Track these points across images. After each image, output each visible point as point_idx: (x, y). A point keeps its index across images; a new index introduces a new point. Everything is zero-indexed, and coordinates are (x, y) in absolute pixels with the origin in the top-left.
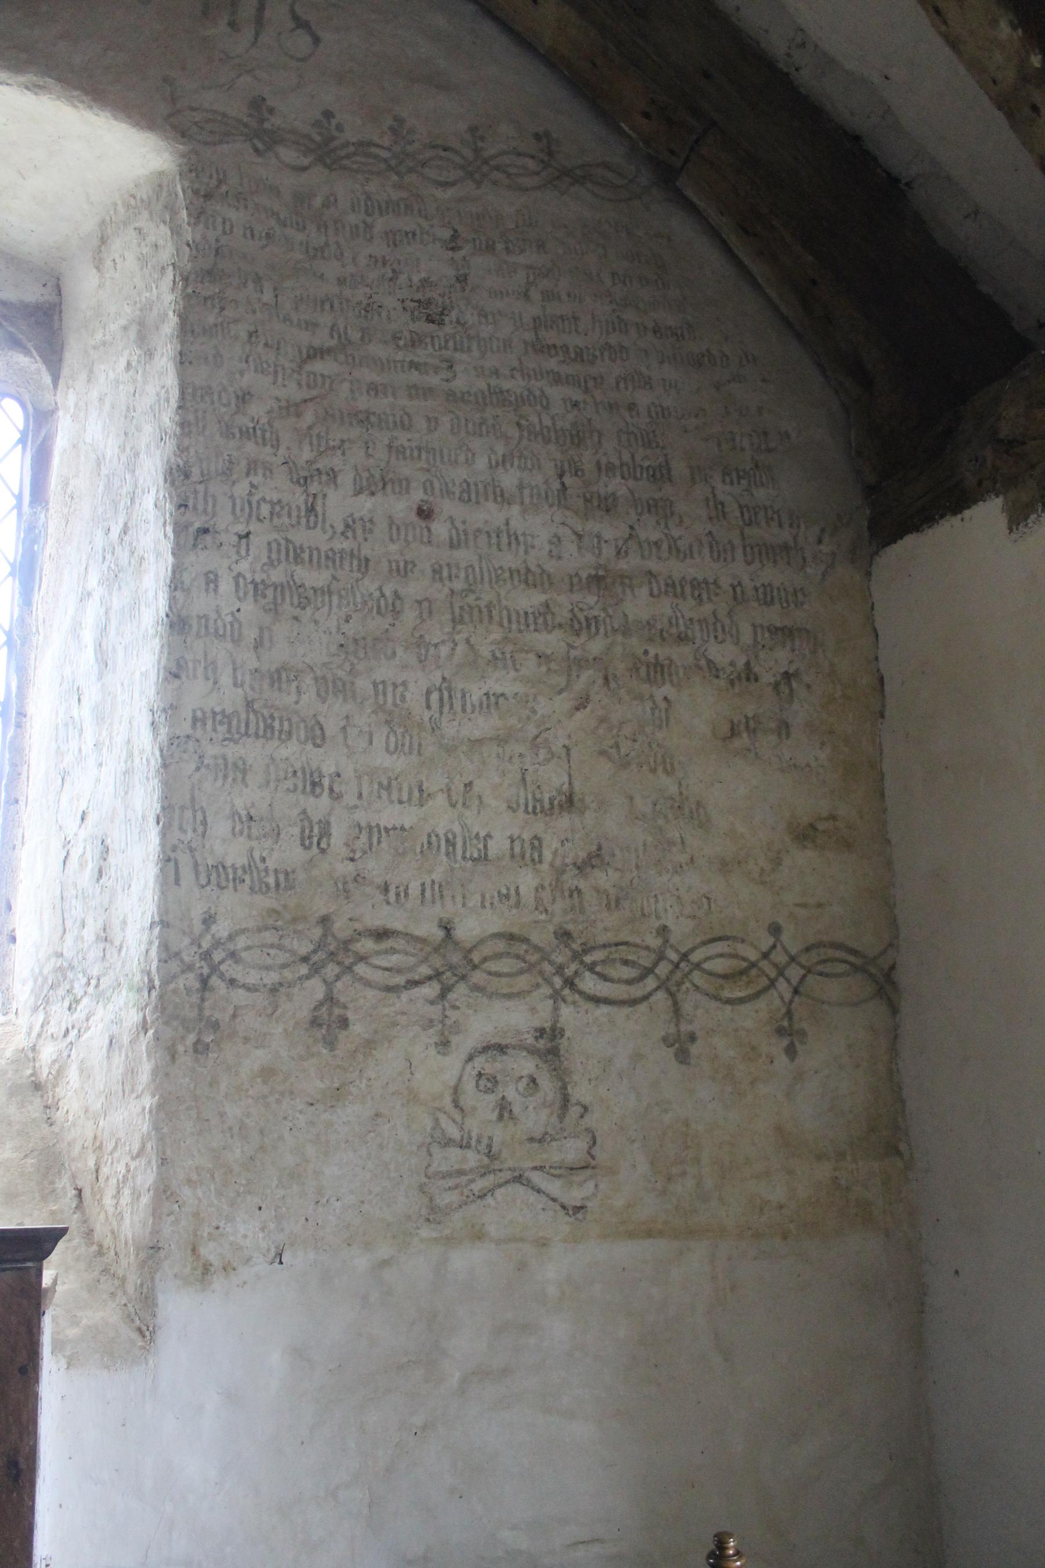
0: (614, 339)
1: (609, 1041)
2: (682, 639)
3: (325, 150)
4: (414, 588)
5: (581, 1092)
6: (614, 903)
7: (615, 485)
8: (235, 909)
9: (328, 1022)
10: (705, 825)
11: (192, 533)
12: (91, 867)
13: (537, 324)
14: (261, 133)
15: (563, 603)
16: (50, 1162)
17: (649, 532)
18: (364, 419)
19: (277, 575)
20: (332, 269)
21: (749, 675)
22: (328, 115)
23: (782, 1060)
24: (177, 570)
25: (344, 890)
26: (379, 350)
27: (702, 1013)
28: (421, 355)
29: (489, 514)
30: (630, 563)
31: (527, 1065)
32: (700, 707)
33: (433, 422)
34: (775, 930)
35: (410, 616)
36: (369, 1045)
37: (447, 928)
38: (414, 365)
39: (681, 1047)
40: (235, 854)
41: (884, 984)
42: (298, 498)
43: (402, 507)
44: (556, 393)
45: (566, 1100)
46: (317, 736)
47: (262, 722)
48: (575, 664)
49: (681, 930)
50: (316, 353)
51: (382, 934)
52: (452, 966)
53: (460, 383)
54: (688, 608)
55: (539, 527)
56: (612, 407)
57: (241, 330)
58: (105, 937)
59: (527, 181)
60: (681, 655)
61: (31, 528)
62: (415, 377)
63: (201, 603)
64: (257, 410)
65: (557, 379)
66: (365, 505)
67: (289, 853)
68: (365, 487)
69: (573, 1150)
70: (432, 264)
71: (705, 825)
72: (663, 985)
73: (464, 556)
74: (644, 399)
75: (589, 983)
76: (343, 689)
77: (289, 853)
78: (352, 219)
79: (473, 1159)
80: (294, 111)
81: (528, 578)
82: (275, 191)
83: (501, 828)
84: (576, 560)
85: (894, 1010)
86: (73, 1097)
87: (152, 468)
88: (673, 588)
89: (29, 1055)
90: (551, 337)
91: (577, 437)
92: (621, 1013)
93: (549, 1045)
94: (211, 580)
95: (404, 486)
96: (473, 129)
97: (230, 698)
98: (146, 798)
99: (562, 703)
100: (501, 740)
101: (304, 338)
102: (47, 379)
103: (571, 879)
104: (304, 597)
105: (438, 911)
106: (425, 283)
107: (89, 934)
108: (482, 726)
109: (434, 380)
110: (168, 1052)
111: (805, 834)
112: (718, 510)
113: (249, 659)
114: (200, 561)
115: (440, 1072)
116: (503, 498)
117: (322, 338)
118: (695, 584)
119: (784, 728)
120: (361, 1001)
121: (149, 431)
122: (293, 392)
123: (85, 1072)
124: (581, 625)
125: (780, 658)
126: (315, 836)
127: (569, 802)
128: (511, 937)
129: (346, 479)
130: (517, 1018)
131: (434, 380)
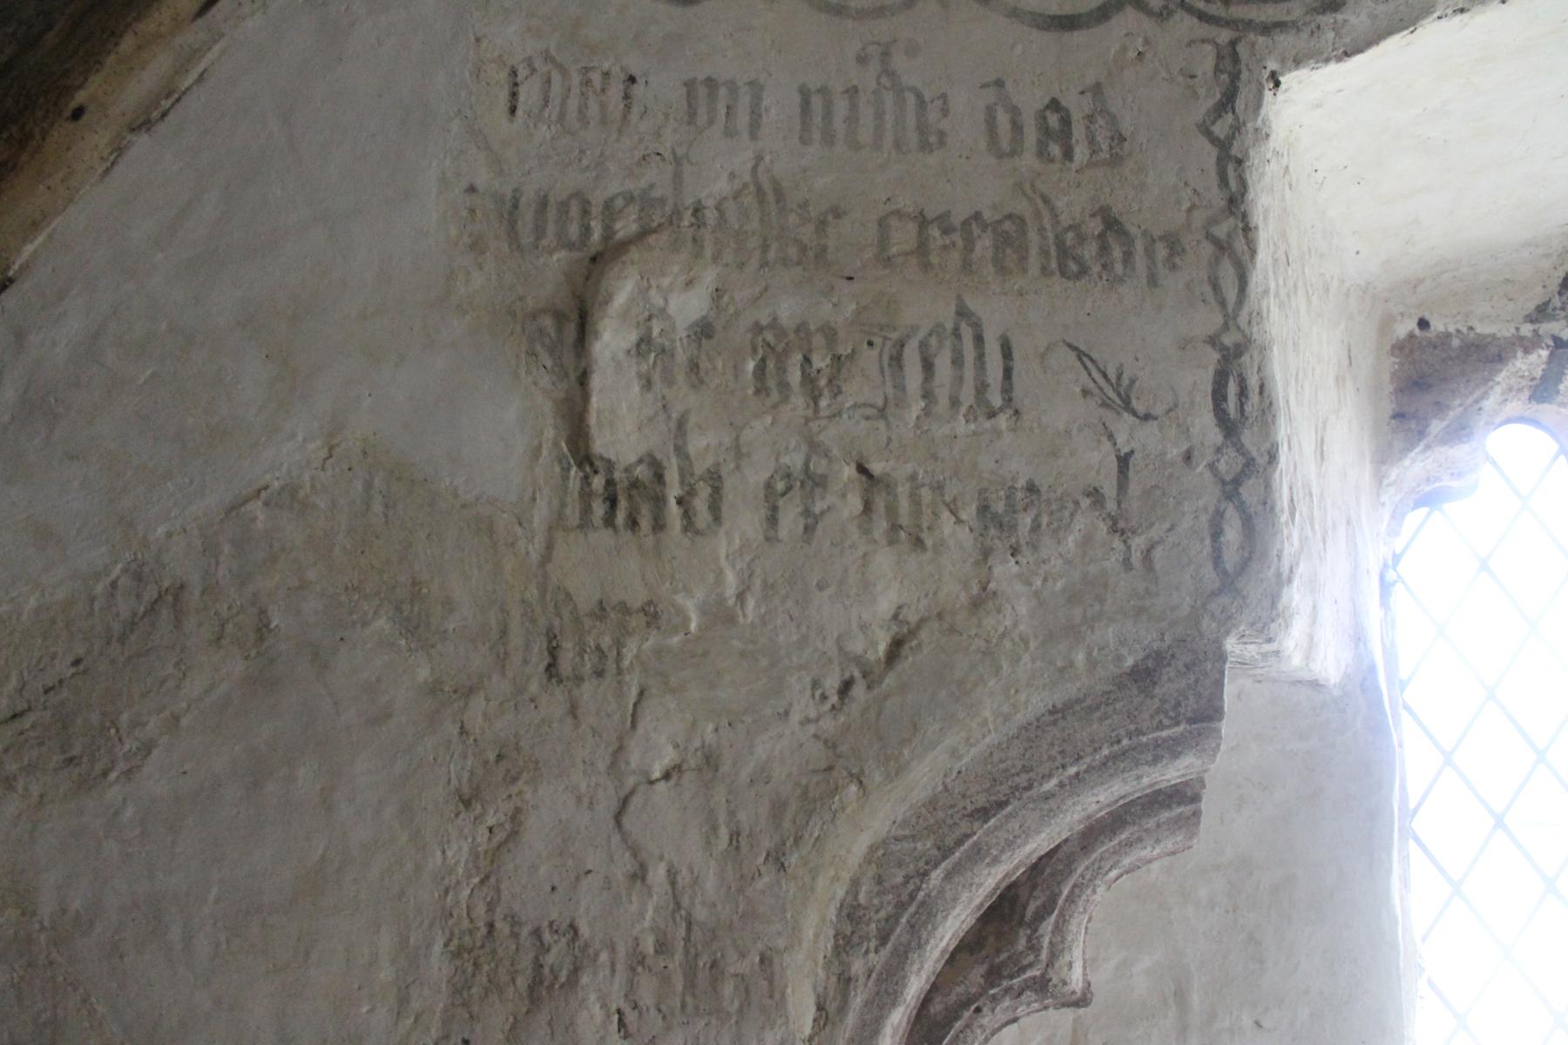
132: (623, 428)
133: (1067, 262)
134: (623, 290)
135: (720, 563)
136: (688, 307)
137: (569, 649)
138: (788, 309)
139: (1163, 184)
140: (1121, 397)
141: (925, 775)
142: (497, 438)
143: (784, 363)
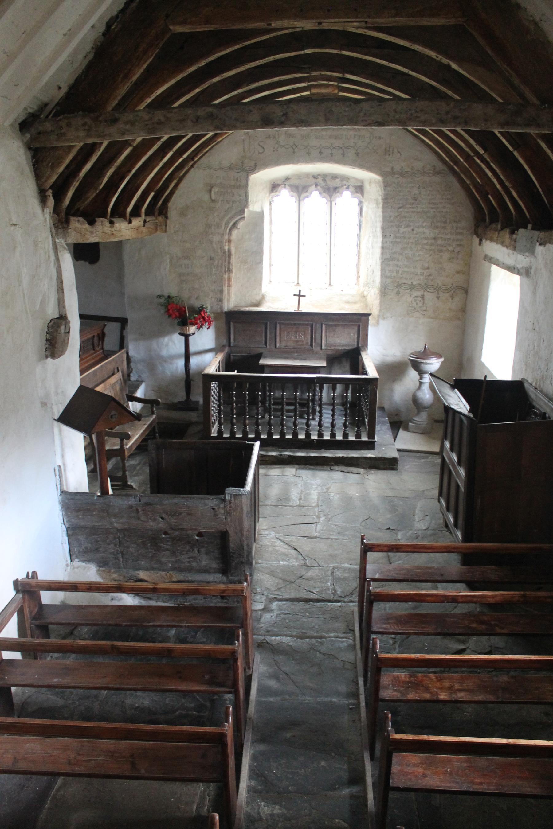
0: (441, 201)
1: (430, 297)
2: (445, 246)
3: (402, 175)
4: (411, 241)
5: (426, 302)
6: (432, 280)
7: (439, 224)
8: (389, 281)
9: (398, 293)
10: (445, 271)
11: (384, 236)
12: (371, 272)
14: (393, 173)
15: (430, 242)
16: (366, 306)
17: (442, 231)
19: (394, 240)
20: (402, 194)
21: (454, 251)
22: (402, 167)
23: (451, 300)
24: (383, 241)
25: (401, 278)
26: (408, 206)
27: (441, 294)
28: (414, 206)
29: (421, 230)
30: (440, 236)
31: (420, 299)
32: (446, 256)
33: (414, 217)
34: (452, 284)
35: (410, 244)
36: (402, 296)
37: (412, 283)
38: (413, 208)
39: (438, 298)
40: (389, 275)
41: (466, 291)
42: (397, 230)
43: (410, 229)
45: (424, 303)
46: (398, 260)
47: (392, 259)
48: (430, 250)
49: (440, 284)
50: (400, 208)
51: (404, 284)
52: (412, 287)
53: (419, 210)
54: (446, 242)
55: (427, 231)
56: (440, 212)
57: (390, 207)
58: (373, 281)
59: (431, 175)
60: (445, 249)
61: (360, 220)
62: (413, 210)
63: (385, 245)
64: (392, 218)
65: (432, 208)
66: (405, 230)
67: (394, 274)
68: (406, 227)
69: (424, 308)
71: (445, 271)
72: (437, 291)
73: (417, 236)
74: (444, 210)
75: (428, 290)
76: (401, 254)
77: (394, 274)
78: (405, 185)
79: (413, 309)
80: (397, 168)
81: (426, 238)
82: (394, 183)
83: (419, 271)
84: (432, 236)
85: (467, 295)
86: (369, 299)
87: (379, 225)
88: (445, 240)
89: (363, 293)
90: (432, 201)
91: (434, 217)
92: (431, 294)
93: (423, 297)
94: (386, 242)
95: (410, 226)
96: (423, 167)
97: (388, 256)
98: (379, 267)
99: (428, 255)
100: (420, 260)
101: (399, 206)
102: (362, 197)
103: (427, 278)
104: (397, 243)
105: (411, 281)
106: (415, 194)
107: (371, 280)
108: (418, 258)
109: (415, 210)
110: (381, 296)
111: (458, 272)
112: (453, 227)
113: (391, 251)
114: (385, 240)
115: (410, 299)
116: (423, 227)
117: (401, 205)
118: (448, 239)
119: (457, 258)
120: (401, 291)
121: (378, 219)
122: (396, 214)
123: (371, 296)
124: (432, 245)
125: (458, 249)
126: (398, 272)
127: (428, 268)
128: (419, 284)
129: (403, 227)
130: (419, 293)
131: (415, 210)
132: (213, 197)
134: (213, 189)
135: (219, 205)
136: (216, 190)
137: (211, 209)
138: (222, 190)
140: (240, 196)
141: (229, 216)
142: (206, 197)
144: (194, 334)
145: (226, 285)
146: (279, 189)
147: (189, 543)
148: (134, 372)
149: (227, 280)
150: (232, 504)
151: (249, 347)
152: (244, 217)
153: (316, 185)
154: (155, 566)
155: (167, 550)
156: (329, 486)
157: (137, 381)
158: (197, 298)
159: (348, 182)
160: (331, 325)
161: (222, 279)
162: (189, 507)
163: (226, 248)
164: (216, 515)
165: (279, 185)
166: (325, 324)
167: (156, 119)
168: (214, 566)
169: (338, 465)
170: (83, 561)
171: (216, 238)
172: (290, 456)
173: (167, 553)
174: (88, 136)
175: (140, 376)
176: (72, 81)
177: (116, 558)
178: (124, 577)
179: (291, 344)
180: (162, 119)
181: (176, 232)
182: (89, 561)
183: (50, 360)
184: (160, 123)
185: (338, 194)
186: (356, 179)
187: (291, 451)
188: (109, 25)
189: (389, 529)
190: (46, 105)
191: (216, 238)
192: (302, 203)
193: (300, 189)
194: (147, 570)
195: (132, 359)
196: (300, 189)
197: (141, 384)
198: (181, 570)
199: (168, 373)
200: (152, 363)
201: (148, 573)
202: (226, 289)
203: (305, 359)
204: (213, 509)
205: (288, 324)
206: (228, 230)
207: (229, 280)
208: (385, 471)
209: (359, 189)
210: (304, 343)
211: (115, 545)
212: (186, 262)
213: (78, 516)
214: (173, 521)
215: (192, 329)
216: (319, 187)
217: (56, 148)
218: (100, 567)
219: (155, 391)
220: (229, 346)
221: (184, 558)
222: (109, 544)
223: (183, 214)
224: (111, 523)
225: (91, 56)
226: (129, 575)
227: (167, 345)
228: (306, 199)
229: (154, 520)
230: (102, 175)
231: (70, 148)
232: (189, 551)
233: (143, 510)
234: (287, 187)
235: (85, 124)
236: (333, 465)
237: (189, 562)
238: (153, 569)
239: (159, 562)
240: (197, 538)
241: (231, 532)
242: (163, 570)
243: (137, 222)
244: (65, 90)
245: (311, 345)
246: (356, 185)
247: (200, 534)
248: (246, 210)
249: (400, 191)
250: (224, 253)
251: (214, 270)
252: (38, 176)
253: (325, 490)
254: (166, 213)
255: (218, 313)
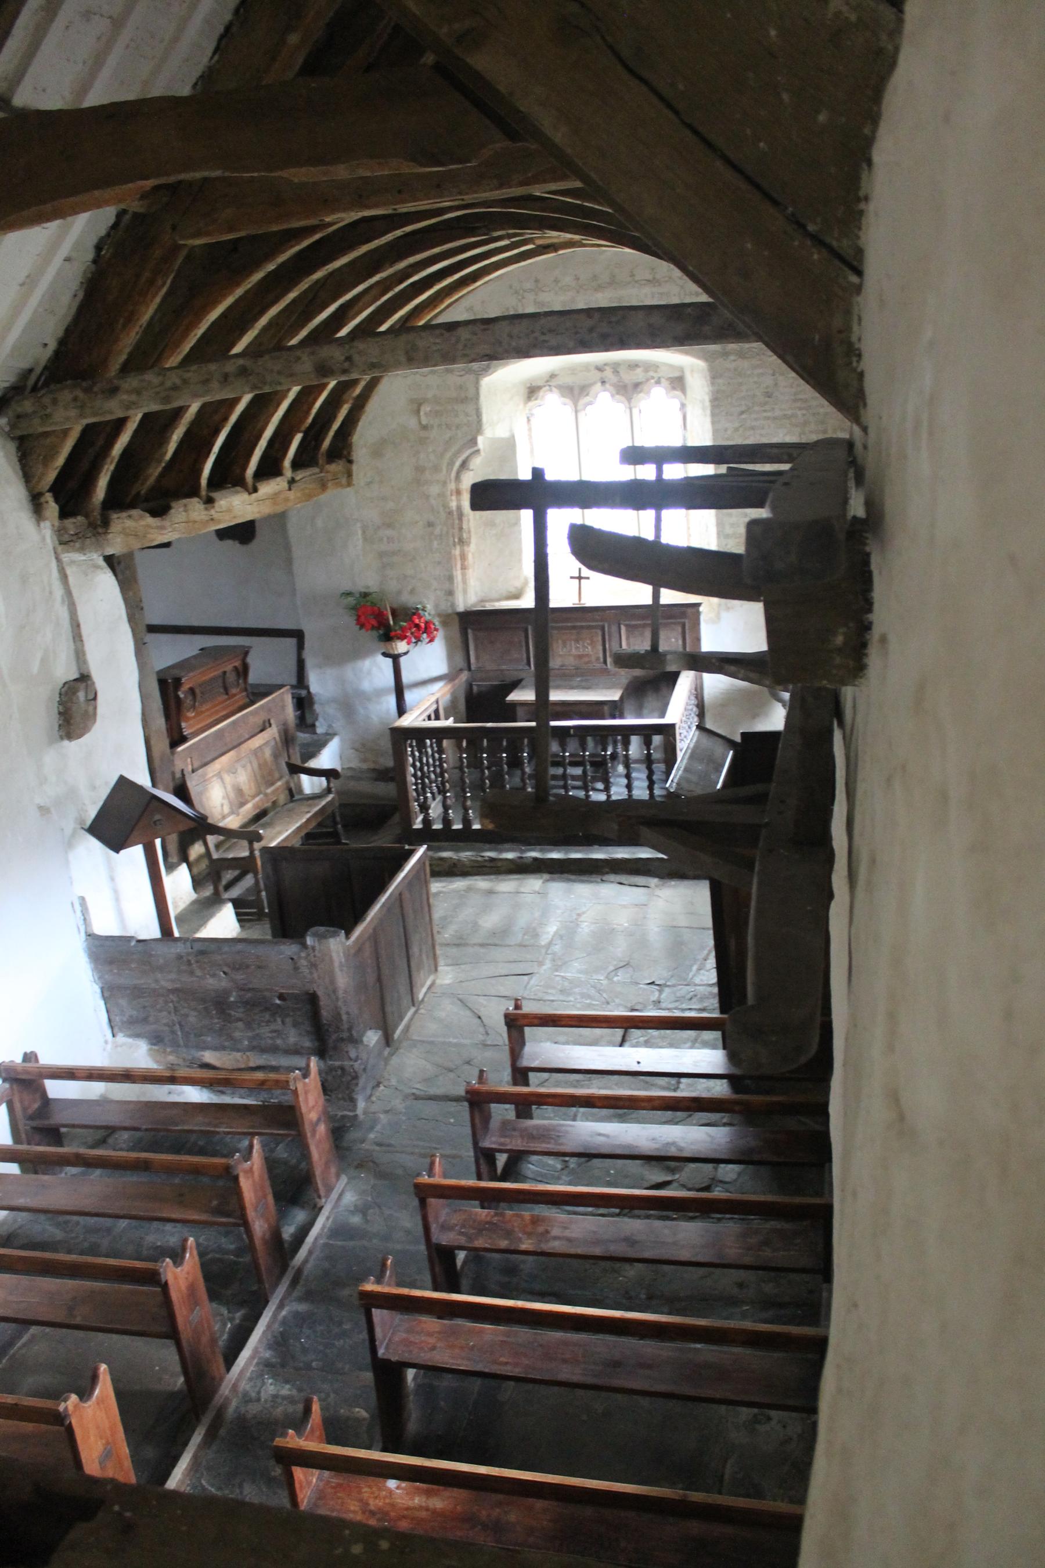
13: (795, 394)
18: (753, 428)
26: (756, 408)
28: (767, 407)
38: (765, 411)
44: (799, 413)
50: (742, 413)
53: (778, 413)
62: (765, 414)
64: (729, 432)
65: (800, 409)
70: (768, 381)
74: (822, 410)
91: (806, 423)
109: (769, 414)
117: (743, 408)
122: (737, 425)
131: (769, 414)
133: (462, 402)
135: (434, 433)
136: (428, 409)
137: (422, 441)
139: (471, 392)
140: (467, 415)
142: (413, 423)
143: (437, 414)
144: (406, 653)
145: (459, 566)
146: (541, 393)
147: (267, 1009)
148: (321, 719)
149: (458, 558)
150: (316, 953)
151: (502, 671)
152: (478, 451)
153: (603, 382)
154: (226, 1044)
155: (241, 1020)
156: (584, 909)
157: (327, 734)
158: (412, 592)
159: (656, 372)
160: (635, 627)
161: (449, 558)
162: (258, 957)
163: (453, 504)
164: (296, 968)
165: (539, 388)
166: (626, 626)
167: (169, 384)
168: (307, 1043)
169: (616, 873)
170: (130, 1036)
171: (434, 490)
172: (535, 859)
173: (240, 1024)
174: (82, 416)
175: (330, 726)
176: (60, 333)
177: (173, 1032)
178: (184, 1059)
179: (570, 661)
180: (178, 381)
181: (369, 484)
182: (137, 1036)
183: (66, 743)
184: (175, 388)
185: (642, 395)
186: (671, 366)
187: (541, 851)
188: (98, 248)
189: (653, 983)
190: (30, 371)
191: (434, 490)
192: (581, 415)
193: (576, 392)
194: (215, 1049)
195: (316, 699)
196: (576, 392)
197: (332, 739)
198: (263, 1050)
199: (375, 719)
200: (349, 704)
201: (217, 1054)
202: (458, 574)
203: (587, 688)
204: (292, 959)
205: (562, 628)
206: (453, 474)
207: (463, 557)
208: (696, 882)
209: (678, 383)
210: (593, 659)
211: (170, 1013)
212: (389, 532)
213: (111, 971)
214: (239, 976)
215: (401, 646)
216: (607, 386)
217: (46, 434)
218: (153, 1044)
219: (357, 750)
220: (469, 669)
221: (265, 1031)
222: (160, 1011)
223: (377, 452)
224: (157, 981)
225: (81, 295)
226: (190, 1057)
227: (369, 673)
228: (589, 408)
229: (214, 976)
230: (164, 441)
231: (65, 433)
232: (269, 1021)
233: (197, 962)
234: (554, 389)
235: (75, 399)
236: (607, 873)
237: (271, 1038)
238: (223, 1048)
239: (230, 1038)
240: (278, 1002)
241: (320, 993)
242: (238, 1051)
243: (268, 488)
244: (52, 346)
245: (605, 662)
246: (671, 375)
247: (281, 997)
248: (480, 439)
249: (741, 384)
250: (450, 513)
251: (435, 543)
252: (27, 476)
253: (575, 917)
254: (349, 453)
255: (448, 615)
